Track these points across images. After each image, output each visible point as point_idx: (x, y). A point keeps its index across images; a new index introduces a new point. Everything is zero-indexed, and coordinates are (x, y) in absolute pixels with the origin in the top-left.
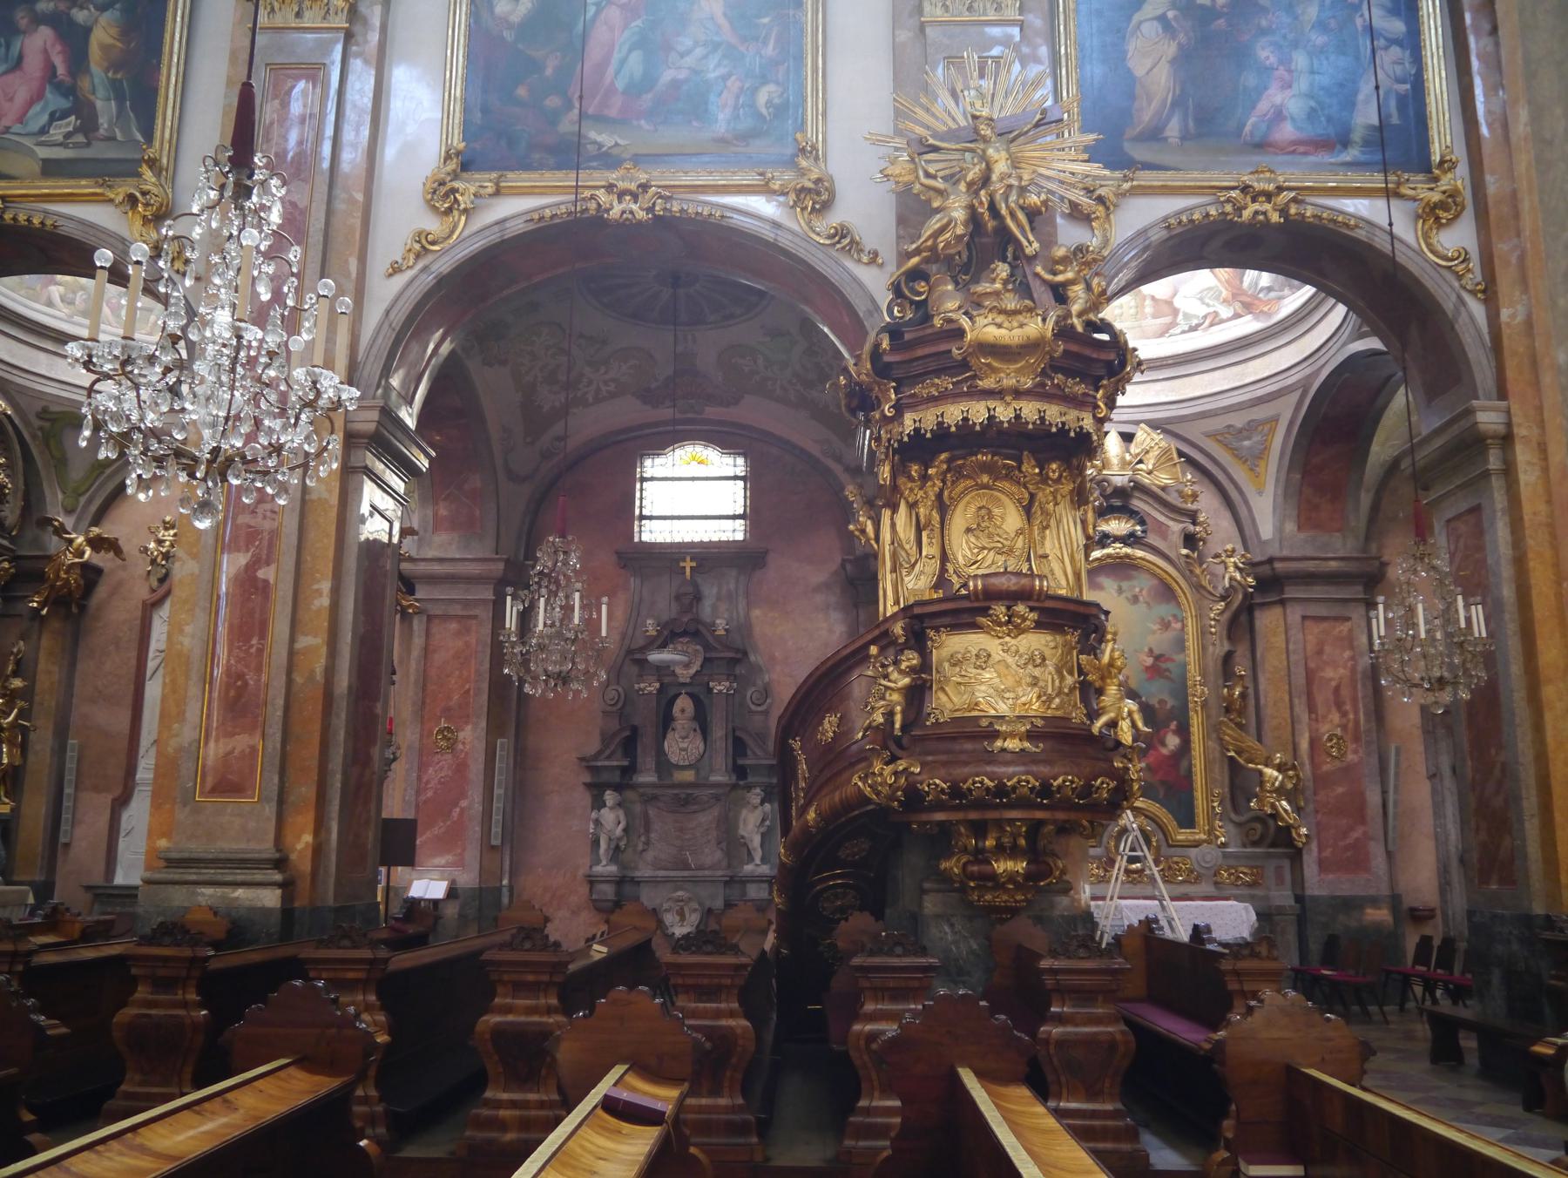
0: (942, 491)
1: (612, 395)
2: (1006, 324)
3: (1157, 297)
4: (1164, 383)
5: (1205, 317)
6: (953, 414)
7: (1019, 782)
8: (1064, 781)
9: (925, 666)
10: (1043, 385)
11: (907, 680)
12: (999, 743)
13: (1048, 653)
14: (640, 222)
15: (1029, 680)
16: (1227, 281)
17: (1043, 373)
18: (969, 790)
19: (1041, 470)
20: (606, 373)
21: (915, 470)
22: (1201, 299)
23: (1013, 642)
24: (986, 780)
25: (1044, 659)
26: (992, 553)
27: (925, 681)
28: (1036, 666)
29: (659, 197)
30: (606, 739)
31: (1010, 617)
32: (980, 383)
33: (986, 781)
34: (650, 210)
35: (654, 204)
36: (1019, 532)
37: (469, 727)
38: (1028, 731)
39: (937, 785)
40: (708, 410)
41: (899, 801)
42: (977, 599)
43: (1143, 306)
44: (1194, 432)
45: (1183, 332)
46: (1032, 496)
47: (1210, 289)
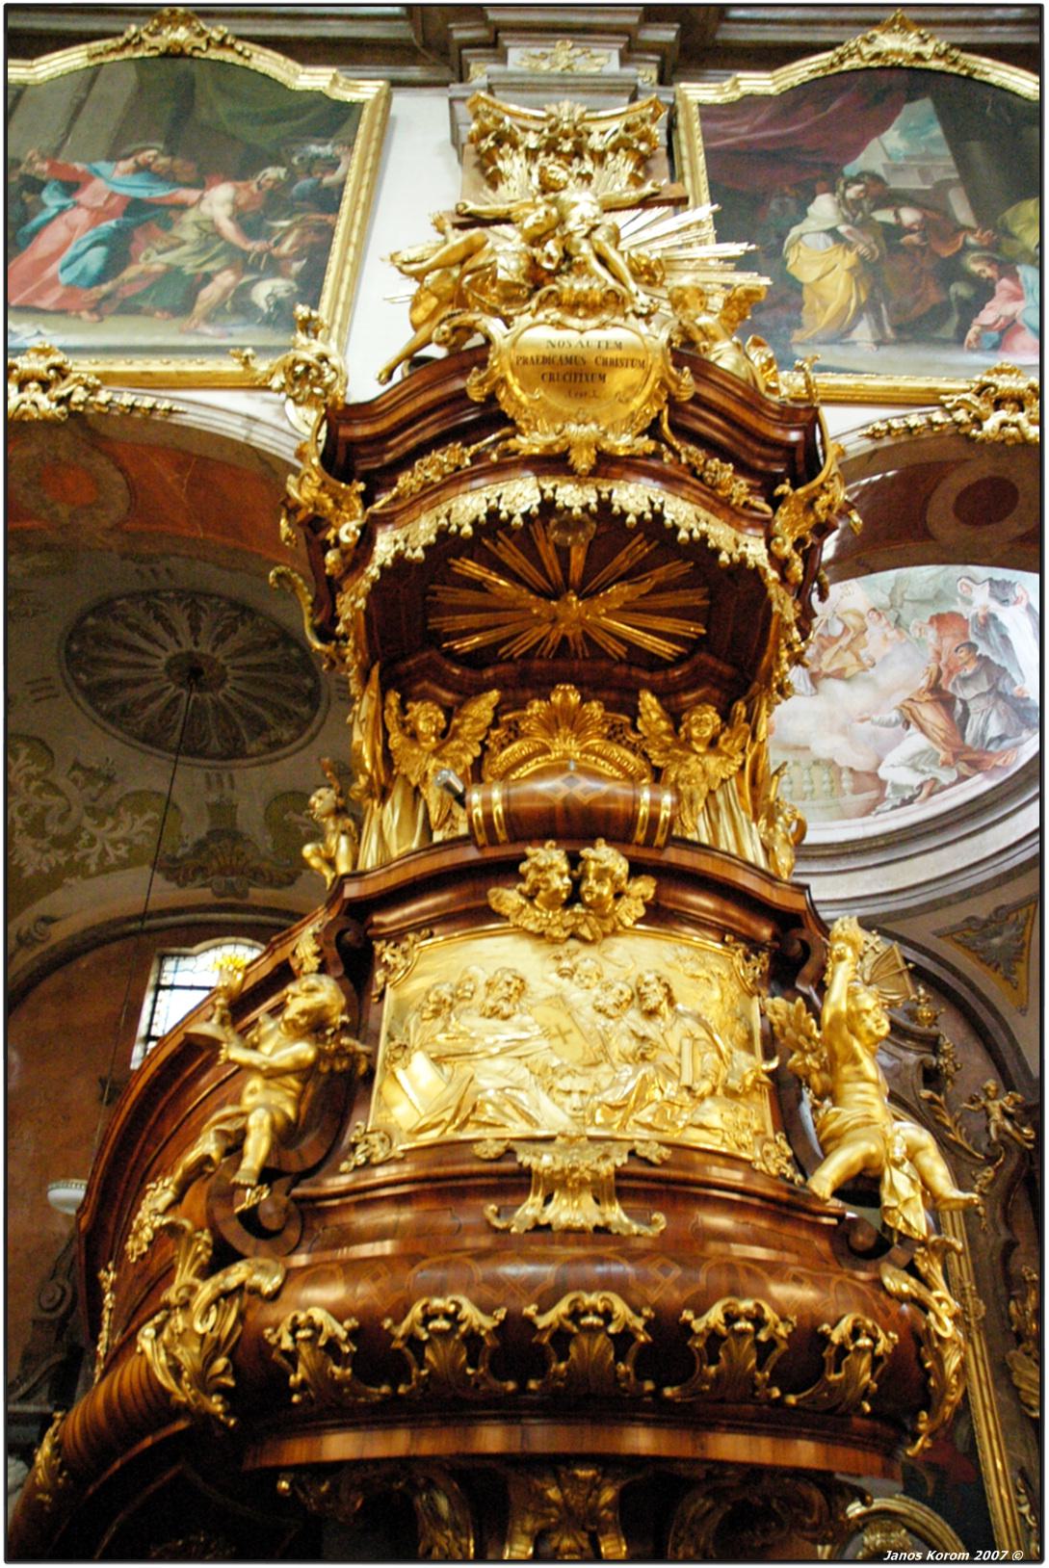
1: (124, 864)
3: (856, 768)
4: (875, 871)
5: (921, 786)
6: (468, 507)
7: (575, 1315)
9: (360, 1023)
11: (305, 1050)
12: (531, 1209)
15: (630, 1045)
16: (945, 741)
17: (653, 430)
18: (411, 1339)
21: (426, 717)
22: (914, 768)
24: (469, 1310)
27: (353, 1057)
33: (469, 1310)
38: (620, 1174)
39: (317, 1329)
40: (252, 891)
41: (222, 1390)
42: (493, 841)
43: (840, 781)
44: (922, 930)
45: (895, 807)
47: (923, 752)
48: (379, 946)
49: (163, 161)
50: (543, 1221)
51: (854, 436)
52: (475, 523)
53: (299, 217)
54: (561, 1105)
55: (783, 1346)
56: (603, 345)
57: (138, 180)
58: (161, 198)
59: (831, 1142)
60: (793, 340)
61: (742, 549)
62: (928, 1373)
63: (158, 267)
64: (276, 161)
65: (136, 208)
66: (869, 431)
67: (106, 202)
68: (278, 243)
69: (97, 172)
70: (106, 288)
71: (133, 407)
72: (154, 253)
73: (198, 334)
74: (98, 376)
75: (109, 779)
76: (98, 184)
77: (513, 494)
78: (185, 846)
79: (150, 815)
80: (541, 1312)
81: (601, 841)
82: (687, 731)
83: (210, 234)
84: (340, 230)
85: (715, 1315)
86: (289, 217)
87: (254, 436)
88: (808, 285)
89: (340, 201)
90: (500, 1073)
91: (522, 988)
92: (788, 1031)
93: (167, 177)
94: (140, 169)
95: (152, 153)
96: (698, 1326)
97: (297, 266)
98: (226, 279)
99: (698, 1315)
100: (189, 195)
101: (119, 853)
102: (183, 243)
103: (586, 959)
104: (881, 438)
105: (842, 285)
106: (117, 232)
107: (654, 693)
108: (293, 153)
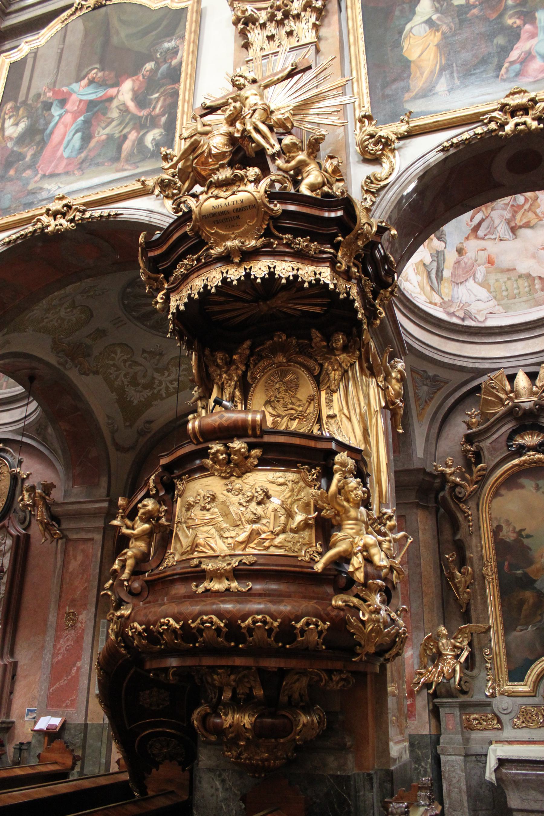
0: (245, 373)
2: (222, 194)
8: (254, 622)
10: (270, 245)
12: (206, 585)
13: (273, 489)
14: (67, 230)
17: (268, 234)
18: (159, 632)
19: (328, 343)
20: (169, 375)
21: (220, 357)
23: (239, 481)
24: (172, 622)
25: (268, 496)
26: (285, 419)
28: (259, 503)
29: (79, 211)
31: (229, 455)
32: (212, 251)
34: (72, 221)
35: (74, 217)
36: (311, 399)
37: (85, 612)
38: (234, 570)
39: (136, 628)
46: (321, 366)
48: (175, 481)
49: (100, 74)
50: (208, 588)
51: (434, 152)
52: (199, 293)
53: (162, 90)
54: (224, 542)
55: (275, 630)
56: (235, 203)
57: (90, 90)
58: (101, 97)
59: (334, 545)
60: (405, 99)
61: (318, 276)
62: (354, 634)
63: (104, 137)
64: (149, 58)
65: (91, 105)
66: (441, 147)
67: (78, 106)
68: (154, 108)
69: (72, 90)
70: (83, 155)
71: (101, 216)
72: (101, 130)
73: (125, 170)
74: (84, 204)
75: (161, 354)
76: (74, 97)
77: (212, 277)
80: (193, 622)
81: (235, 439)
82: (332, 345)
83: (124, 110)
84: (181, 92)
85: (250, 620)
86: (157, 92)
87: (152, 220)
88: (414, 61)
89: (180, 74)
90: (205, 532)
91: (213, 498)
92: (319, 502)
93: (103, 84)
94: (91, 82)
95: (95, 71)
96: (243, 625)
97: (163, 119)
98: (133, 136)
99: (243, 621)
100: (112, 91)
101: (174, 386)
102: (113, 120)
103: (238, 483)
104: (448, 150)
105: (432, 56)
106: (85, 122)
107: (317, 329)
108: (157, 51)
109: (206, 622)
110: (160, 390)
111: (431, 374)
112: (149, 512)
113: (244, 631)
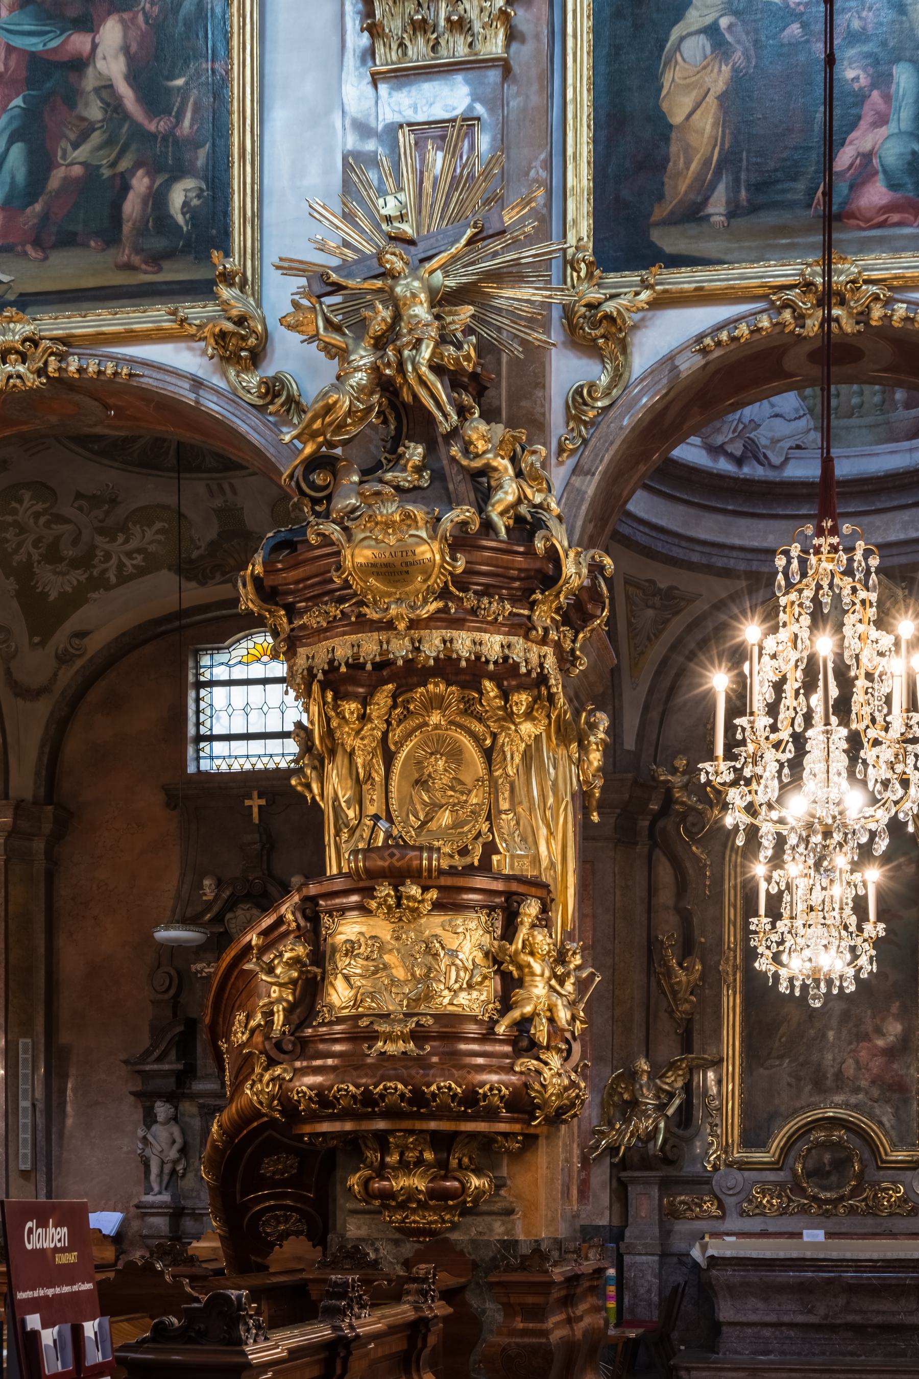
1: (142, 572)
7: (386, 1088)
30: (157, 1032)
78: (198, 548)
79: (158, 525)
101: (135, 562)
109: (390, 1088)
110: (106, 570)
111: (663, 585)
112: (298, 956)
113: (429, 1096)
